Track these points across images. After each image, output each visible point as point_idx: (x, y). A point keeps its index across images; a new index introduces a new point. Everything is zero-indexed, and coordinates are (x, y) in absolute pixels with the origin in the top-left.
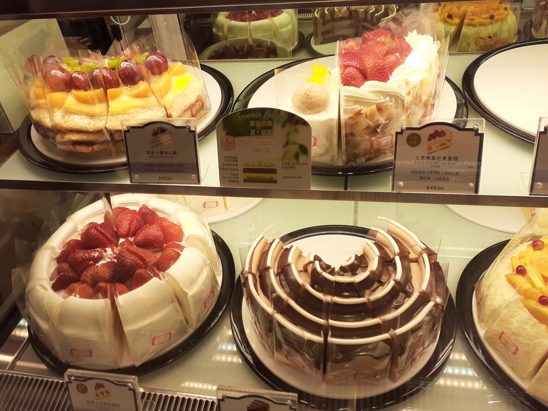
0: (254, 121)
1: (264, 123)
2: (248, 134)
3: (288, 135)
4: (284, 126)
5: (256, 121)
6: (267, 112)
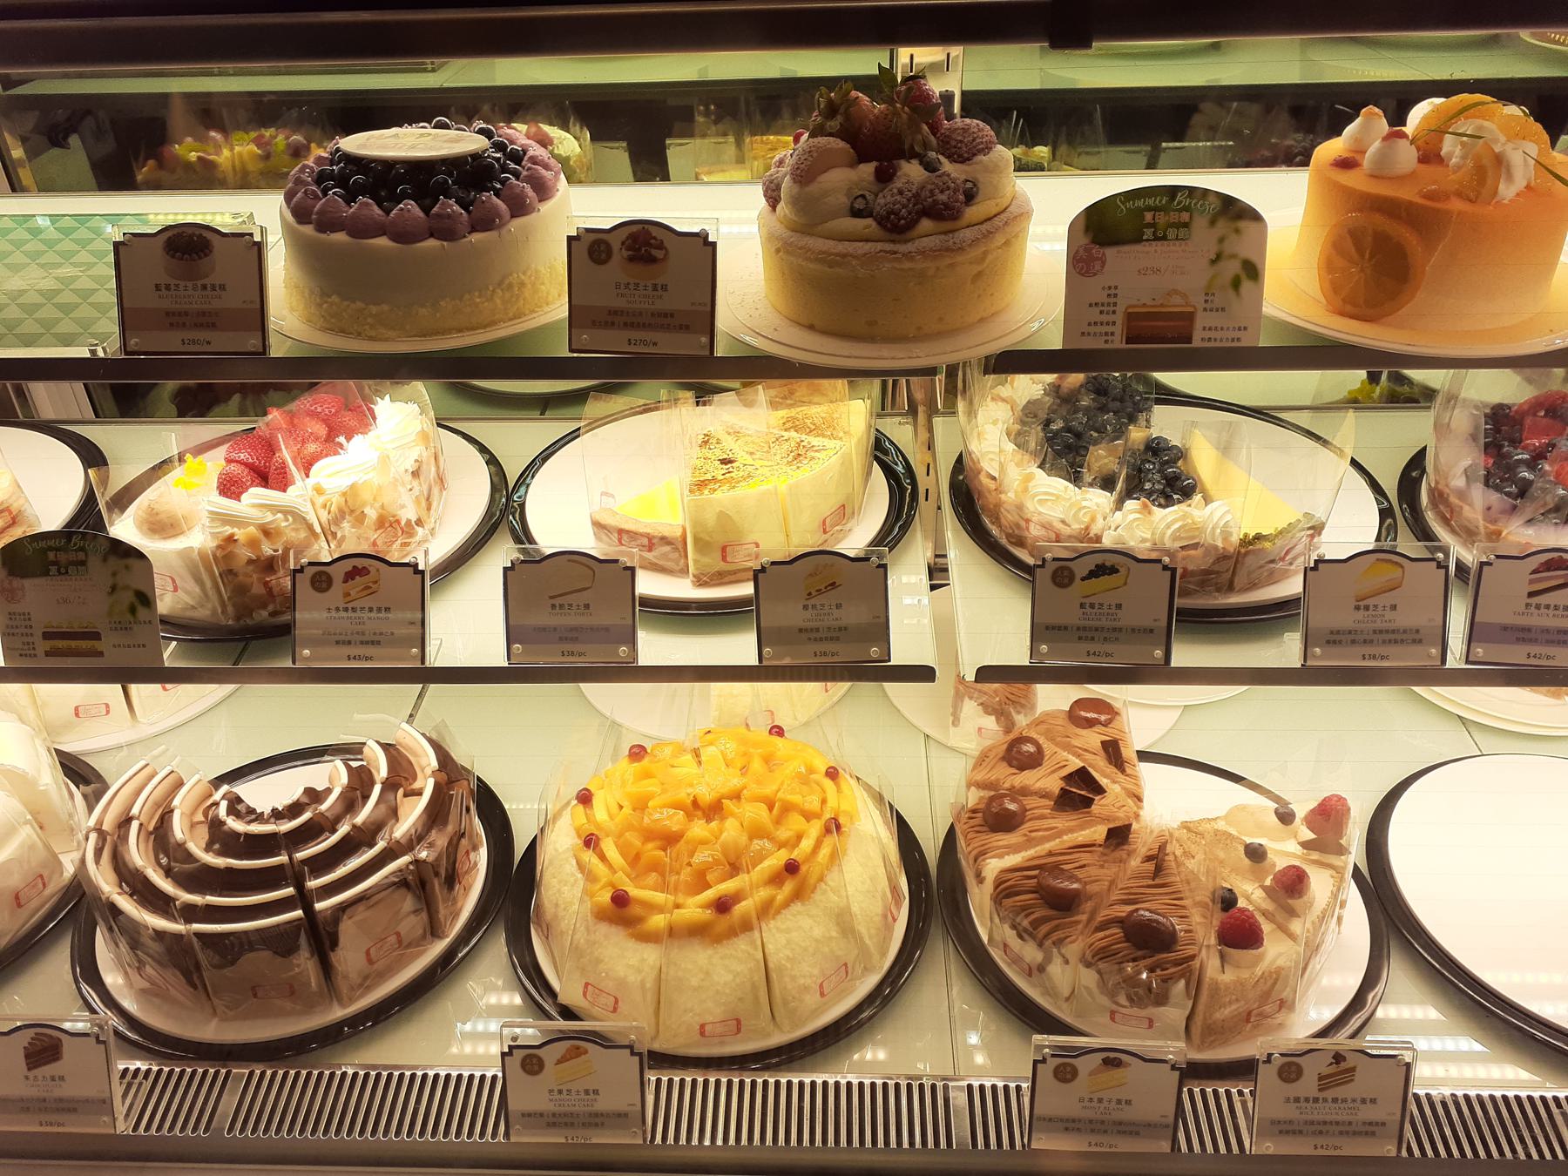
0: (1153, 213)
1: (1173, 217)
2: (1138, 239)
3: (1221, 240)
4: (1213, 222)
5: (1157, 213)
6: (1180, 194)
